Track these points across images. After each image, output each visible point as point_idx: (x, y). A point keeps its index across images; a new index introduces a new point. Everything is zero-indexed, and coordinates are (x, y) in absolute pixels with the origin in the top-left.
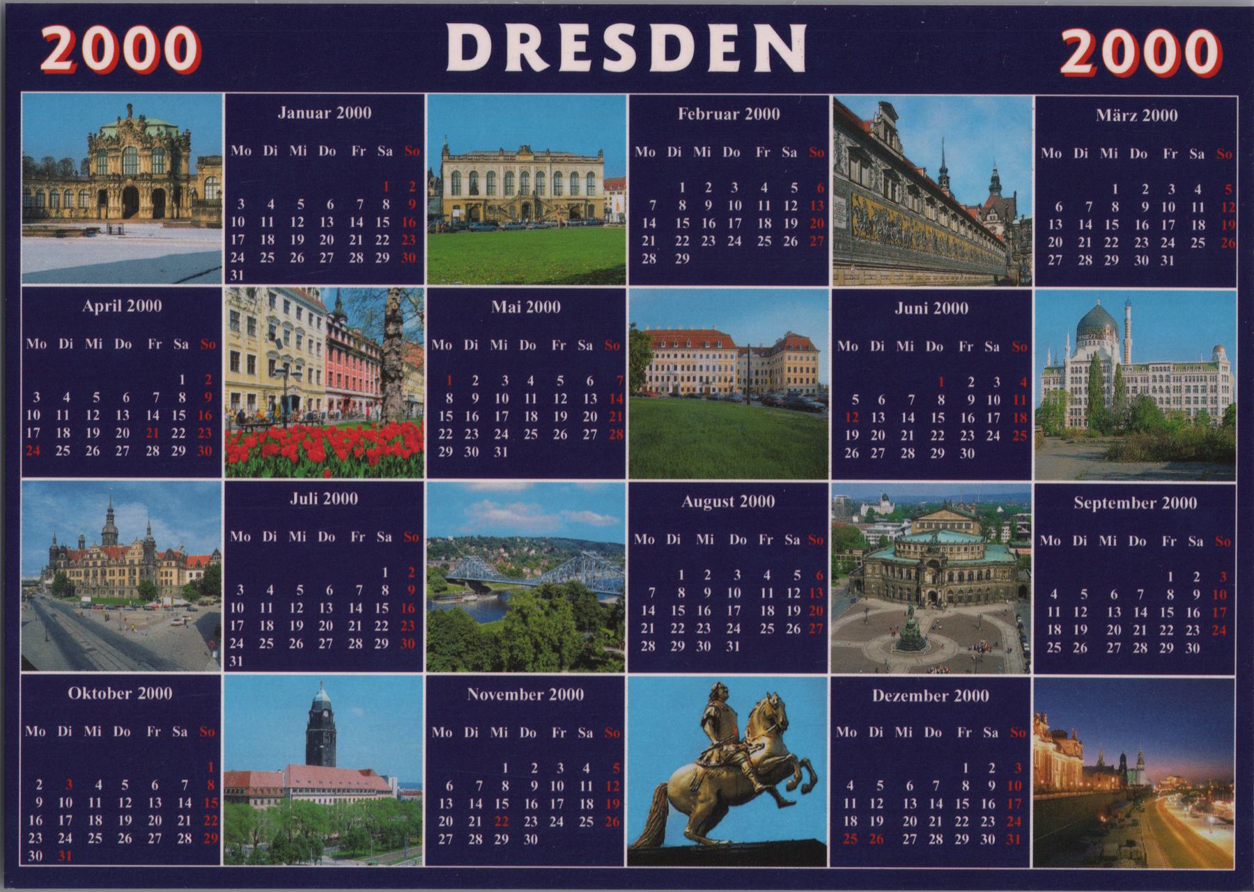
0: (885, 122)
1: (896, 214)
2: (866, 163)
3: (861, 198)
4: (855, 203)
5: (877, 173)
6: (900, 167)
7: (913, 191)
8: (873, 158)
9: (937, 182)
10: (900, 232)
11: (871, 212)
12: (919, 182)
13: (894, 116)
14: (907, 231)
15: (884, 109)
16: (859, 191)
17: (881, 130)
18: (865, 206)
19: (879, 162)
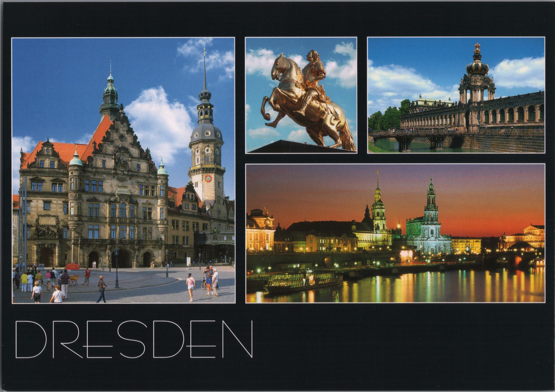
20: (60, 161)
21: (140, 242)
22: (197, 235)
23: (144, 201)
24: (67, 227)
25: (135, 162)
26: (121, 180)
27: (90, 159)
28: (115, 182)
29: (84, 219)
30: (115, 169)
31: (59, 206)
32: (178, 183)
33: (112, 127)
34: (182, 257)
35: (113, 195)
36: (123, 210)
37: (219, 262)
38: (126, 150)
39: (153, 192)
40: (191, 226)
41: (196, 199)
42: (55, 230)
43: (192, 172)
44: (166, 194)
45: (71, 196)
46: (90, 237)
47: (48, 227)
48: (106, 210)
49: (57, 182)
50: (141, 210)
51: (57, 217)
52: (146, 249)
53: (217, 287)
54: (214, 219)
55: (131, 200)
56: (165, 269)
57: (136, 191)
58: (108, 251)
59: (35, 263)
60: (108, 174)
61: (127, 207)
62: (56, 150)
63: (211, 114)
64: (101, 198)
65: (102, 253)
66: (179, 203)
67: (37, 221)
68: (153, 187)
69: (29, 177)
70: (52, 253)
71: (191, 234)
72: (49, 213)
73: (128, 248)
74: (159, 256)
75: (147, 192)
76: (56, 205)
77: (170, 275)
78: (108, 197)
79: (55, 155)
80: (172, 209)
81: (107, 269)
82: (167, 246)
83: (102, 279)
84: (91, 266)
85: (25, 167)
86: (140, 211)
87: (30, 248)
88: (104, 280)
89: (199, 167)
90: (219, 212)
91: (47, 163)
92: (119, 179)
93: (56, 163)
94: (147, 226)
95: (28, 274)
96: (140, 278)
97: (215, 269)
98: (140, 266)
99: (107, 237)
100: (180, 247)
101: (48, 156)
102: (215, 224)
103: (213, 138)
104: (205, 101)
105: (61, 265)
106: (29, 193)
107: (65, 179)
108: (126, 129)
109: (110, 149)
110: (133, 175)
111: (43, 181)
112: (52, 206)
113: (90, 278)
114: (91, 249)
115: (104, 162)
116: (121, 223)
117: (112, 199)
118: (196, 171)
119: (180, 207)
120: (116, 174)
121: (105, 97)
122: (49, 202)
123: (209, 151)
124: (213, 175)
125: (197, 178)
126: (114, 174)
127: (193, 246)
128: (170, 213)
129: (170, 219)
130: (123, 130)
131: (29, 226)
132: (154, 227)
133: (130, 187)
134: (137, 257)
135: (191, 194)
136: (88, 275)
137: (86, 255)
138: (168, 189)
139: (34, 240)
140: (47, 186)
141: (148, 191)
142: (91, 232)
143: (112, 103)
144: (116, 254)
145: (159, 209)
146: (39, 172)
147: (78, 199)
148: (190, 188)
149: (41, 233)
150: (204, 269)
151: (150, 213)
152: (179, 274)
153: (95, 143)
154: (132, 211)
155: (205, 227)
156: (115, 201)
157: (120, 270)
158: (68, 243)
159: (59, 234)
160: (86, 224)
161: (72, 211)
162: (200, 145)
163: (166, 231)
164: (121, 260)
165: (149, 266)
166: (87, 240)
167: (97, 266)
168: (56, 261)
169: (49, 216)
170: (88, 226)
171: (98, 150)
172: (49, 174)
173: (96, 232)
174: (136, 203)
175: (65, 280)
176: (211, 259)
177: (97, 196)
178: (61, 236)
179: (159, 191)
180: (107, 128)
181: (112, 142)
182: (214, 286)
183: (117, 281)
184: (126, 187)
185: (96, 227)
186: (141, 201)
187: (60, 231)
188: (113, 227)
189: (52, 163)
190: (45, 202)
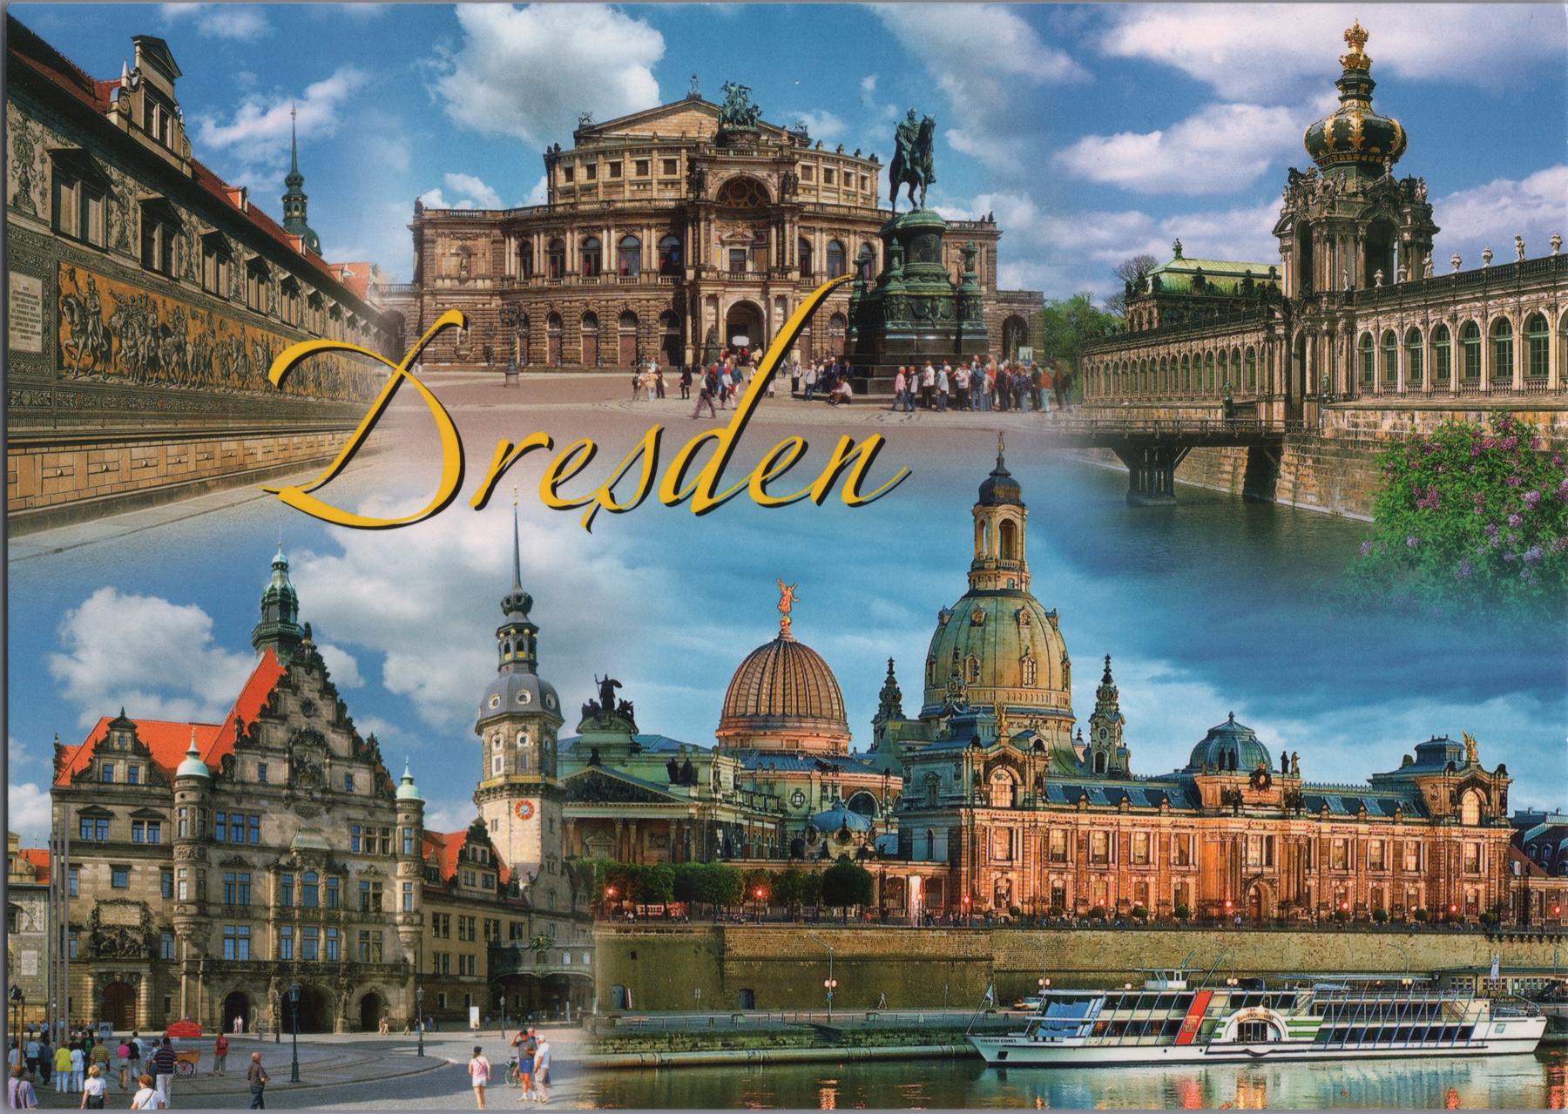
0: (149, 86)
1: (171, 304)
2: (97, 187)
3: (81, 275)
4: (66, 287)
5: (121, 206)
6: (188, 196)
7: (216, 247)
8: (115, 174)
9: (277, 215)
10: (180, 348)
11: (108, 307)
12: (233, 226)
13: (170, 73)
14: (200, 341)
15: (146, 56)
16: (75, 257)
17: (138, 102)
18: (94, 293)
19: (130, 182)
20: (152, 766)
21: (352, 966)
22: (494, 950)
23: (363, 865)
24: (169, 929)
25: (340, 770)
26: (306, 814)
27: (229, 761)
28: (290, 818)
29: (213, 910)
30: (290, 786)
31: (151, 878)
32: (445, 821)
33: (285, 682)
34: (456, 1007)
35: (285, 850)
36: (309, 889)
37: (551, 1018)
38: (319, 740)
39: (385, 843)
40: (479, 927)
41: (495, 862)
42: (140, 939)
43: (480, 796)
44: (419, 851)
45: (180, 853)
46: (228, 956)
47: (122, 930)
48: (267, 888)
49: (145, 817)
50: (354, 889)
51: (144, 906)
52: (367, 987)
53: (547, 1081)
54: (540, 912)
55: (331, 862)
56: (414, 1037)
57: (343, 841)
58: (272, 991)
59: (89, 1020)
60: (275, 798)
61: (321, 881)
62: (142, 739)
63: (532, 649)
64: (256, 859)
65: (258, 996)
66: (450, 872)
67: (96, 914)
68: (385, 832)
69: (74, 807)
70: (133, 994)
71: (480, 949)
72: (126, 895)
73: (323, 984)
74: (399, 1002)
75: (369, 844)
76: (144, 877)
77: (428, 1051)
78: (272, 857)
79: (141, 750)
80: (435, 887)
81: (270, 1037)
82: (421, 979)
83: (257, 1061)
84: (229, 1027)
85: (65, 782)
86: (352, 894)
87: (77, 985)
88: (264, 1064)
89: (501, 781)
90: (552, 893)
91: (120, 771)
92: (300, 812)
93: (142, 770)
94: (371, 928)
95: (72, 1047)
96: (351, 1058)
97: (540, 1035)
98: (353, 1029)
99: (270, 957)
100: (454, 981)
101: (122, 753)
102: (541, 924)
103: (539, 709)
104: (516, 617)
105: (153, 1025)
106: (78, 846)
107: (165, 811)
108: (318, 686)
109: (277, 735)
110: (335, 800)
111: (111, 815)
112: (133, 877)
113: (228, 1061)
114: (230, 986)
115: (263, 769)
116: (304, 922)
117: (283, 861)
118: (492, 792)
119: (454, 881)
120: (294, 798)
121: (266, 606)
122: (127, 868)
123: (527, 740)
124: (536, 802)
125: (496, 811)
126: (288, 798)
127: (485, 980)
128: (427, 895)
129: (428, 910)
130: (310, 690)
131: (76, 928)
132: (387, 931)
133: (328, 831)
134: (346, 1005)
135: (479, 848)
136: (222, 1050)
137: (218, 1001)
138: (426, 839)
139: (87, 962)
140: (120, 828)
141: (374, 840)
142: (229, 944)
143: (284, 621)
144: (294, 998)
145: (399, 884)
146: (101, 794)
147: (199, 860)
148: (478, 833)
149: (103, 945)
150: (513, 1035)
151: (378, 897)
152: (450, 1048)
153: (240, 722)
154: (332, 892)
155: (515, 930)
156: (291, 867)
157: (301, 1038)
158: (173, 970)
159: (151, 946)
160: (218, 924)
161: (184, 891)
162: (505, 728)
163: (417, 942)
164: (304, 1013)
165: (375, 1029)
166: (221, 962)
167: (245, 1029)
168: (142, 1015)
169: (125, 902)
170: (220, 927)
171: (249, 739)
172: (124, 799)
173: (243, 943)
174: (343, 872)
175: (165, 1062)
176: (531, 1011)
177: (244, 853)
178: (154, 954)
179: (400, 839)
180: (271, 683)
181: (284, 718)
182: (539, 1077)
183: (295, 1065)
184: (317, 831)
185: (243, 931)
186: (356, 866)
187: (150, 940)
188: (286, 931)
189: (132, 772)
190: (115, 868)
